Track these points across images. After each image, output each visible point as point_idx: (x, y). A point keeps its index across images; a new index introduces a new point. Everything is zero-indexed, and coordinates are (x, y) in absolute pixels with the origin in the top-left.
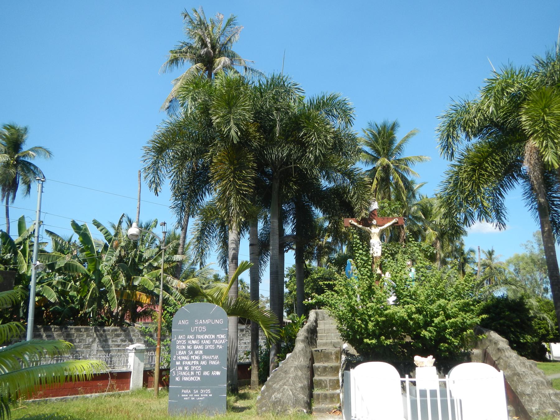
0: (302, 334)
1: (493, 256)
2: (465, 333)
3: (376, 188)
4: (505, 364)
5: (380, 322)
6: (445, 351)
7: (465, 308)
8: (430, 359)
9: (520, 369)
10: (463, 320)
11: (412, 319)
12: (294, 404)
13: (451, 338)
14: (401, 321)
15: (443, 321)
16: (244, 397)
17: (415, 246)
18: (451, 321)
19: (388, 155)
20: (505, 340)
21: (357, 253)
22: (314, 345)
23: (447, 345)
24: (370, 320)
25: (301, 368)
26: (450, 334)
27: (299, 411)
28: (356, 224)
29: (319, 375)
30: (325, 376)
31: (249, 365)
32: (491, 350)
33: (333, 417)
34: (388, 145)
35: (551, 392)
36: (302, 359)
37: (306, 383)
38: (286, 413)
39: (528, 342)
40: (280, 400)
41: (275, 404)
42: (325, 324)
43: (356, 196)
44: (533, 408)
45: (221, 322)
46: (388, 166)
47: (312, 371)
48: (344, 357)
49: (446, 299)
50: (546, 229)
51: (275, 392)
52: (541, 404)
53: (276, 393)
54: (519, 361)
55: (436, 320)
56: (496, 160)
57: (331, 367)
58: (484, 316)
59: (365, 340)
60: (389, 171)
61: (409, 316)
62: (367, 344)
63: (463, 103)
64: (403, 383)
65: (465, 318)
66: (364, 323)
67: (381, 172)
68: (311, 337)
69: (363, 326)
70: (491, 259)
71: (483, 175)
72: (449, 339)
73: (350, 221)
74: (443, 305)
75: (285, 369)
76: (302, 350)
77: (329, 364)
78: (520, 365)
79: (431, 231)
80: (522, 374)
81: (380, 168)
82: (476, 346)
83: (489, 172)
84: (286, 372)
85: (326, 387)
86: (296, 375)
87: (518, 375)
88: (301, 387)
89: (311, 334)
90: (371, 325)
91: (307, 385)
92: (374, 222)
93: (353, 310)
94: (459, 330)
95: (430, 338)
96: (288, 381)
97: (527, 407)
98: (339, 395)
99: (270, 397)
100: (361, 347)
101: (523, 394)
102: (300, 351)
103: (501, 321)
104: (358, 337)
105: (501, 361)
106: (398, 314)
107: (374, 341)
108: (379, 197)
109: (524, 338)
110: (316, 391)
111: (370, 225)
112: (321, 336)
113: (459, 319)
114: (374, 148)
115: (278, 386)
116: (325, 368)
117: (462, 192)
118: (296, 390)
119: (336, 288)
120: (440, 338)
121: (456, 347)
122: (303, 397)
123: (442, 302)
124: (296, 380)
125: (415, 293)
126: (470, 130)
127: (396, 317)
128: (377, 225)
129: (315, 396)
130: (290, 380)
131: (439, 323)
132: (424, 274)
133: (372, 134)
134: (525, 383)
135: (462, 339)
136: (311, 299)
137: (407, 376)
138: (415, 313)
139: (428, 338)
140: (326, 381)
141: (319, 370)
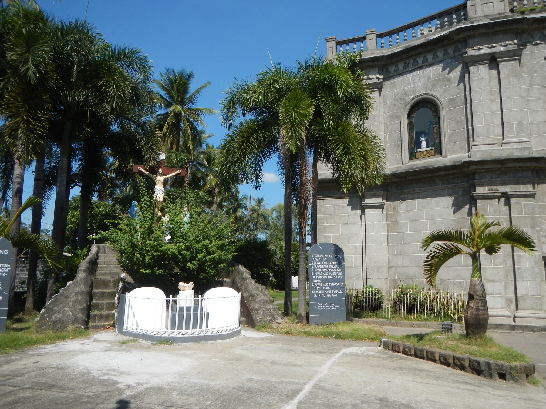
0: (84, 264)
1: (262, 204)
2: (220, 266)
3: (166, 132)
4: (245, 289)
5: (155, 256)
6: (203, 279)
7: (222, 247)
8: (191, 284)
9: (254, 292)
10: (219, 256)
11: (181, 254)
12: (73, 323)
13: (209, 269)
14: (172, 256)
15: (205, 257)
16: (19, 321)
17: (191, 197)
18: (210, 257)
19: (182, 103)
20: (248, 271)
21: (142, 198)
22: (94, 275)
23: (205, 275)
24: (147, 255)
25: (81, 293)
26: (209, 266)
27: (77, 327)
28: (143, 170)
29: (97, 300)
30: (103, 300)
31: (25, 293)
32: (237, 279)
33: (107, 331)
34: (182, 93)
35: (271, 307)
36: (82, 286)
37: (85, 305)
38: (65, 329)
39: (264, 273)
40: (60, 320)
41: (55, 323)
42: (105, 256)
43: (146, 146)
44: (258, 318)
45: (6, 253)
46: (180, 113)
47: (91, 296)
48: (121, 284)
49: (209, 240)
50: (288, 192)
51: (55, 313)
52: (263, 315)
53: (56, 315)
54: (255, 287)
55: (199, 256)
56: (260, 137)
57: (109, 293)
58: (234, 254)
59: (141, 270)
60: (181, 118)
61: (179, 252)
62: (143, 273)
63: (244, 84)
64: (168, 302)
65: (221, 255)
66: (142, 256)
67: (172, 118)
68: (92, 268)
69: (141, 259)
70: (259, 206)
71: (249, 147)
72: (207, 270)
73: (139, 168)
74: (206, 244)
75: (66, 294)
76: (84, 278)
77: (107, 290)
78: (255, 289)
79: (212, 177)
80: (255, 296)
81: (172, 114)
82: (228, 276)
83: (253, 146)
84: (67, 297)
85: (102, 308)
86: (77, 299)
87: (253, 296)
88: (81, 309)
89: (92, 265)
90: (147, 259)
91: (86, 307)
92: (160, 171)
93: (134, 246)
94: (216, 263)
95: (193, 269)
96: (68, 304)
97: (254, 318)
98: (113, 314)
99: (50, 317)
100: (138, 275)
101: (253, 309)
102: (81, 279)
103: (249, 258)
104: (136, 268)
105: (243, 286)
106: (171, 250)
107: (148, 271)
108: (169, 141)
109: (262, 271)
110: (93, 312)
111: (156, 173)
112: (101, 267)
113: (216, 256)
114: (169, 93)
115: (58, 309)
116: (103, 294)
117: (233, 158)
118: (76, 311)
119: (120, 227)
120: (201, 268)
121: (212, 276)
122: (81, 316)
123: (206, 242)
124: (76, 303)
125: (186, 234)
126: (246, 108)
127: (169, 252)
128: (162, 174)
129: (92, 316)
130: (71, 303)
131: (201, 258)
132: (195, 220)
133: (168, 80)
134: (256, 302)
135: (217, 270)
136: (96, 235)
137: (171, 296)
138: (184, 250)
139: (191, 269)
140: (103, 304)
141: (98, 295)
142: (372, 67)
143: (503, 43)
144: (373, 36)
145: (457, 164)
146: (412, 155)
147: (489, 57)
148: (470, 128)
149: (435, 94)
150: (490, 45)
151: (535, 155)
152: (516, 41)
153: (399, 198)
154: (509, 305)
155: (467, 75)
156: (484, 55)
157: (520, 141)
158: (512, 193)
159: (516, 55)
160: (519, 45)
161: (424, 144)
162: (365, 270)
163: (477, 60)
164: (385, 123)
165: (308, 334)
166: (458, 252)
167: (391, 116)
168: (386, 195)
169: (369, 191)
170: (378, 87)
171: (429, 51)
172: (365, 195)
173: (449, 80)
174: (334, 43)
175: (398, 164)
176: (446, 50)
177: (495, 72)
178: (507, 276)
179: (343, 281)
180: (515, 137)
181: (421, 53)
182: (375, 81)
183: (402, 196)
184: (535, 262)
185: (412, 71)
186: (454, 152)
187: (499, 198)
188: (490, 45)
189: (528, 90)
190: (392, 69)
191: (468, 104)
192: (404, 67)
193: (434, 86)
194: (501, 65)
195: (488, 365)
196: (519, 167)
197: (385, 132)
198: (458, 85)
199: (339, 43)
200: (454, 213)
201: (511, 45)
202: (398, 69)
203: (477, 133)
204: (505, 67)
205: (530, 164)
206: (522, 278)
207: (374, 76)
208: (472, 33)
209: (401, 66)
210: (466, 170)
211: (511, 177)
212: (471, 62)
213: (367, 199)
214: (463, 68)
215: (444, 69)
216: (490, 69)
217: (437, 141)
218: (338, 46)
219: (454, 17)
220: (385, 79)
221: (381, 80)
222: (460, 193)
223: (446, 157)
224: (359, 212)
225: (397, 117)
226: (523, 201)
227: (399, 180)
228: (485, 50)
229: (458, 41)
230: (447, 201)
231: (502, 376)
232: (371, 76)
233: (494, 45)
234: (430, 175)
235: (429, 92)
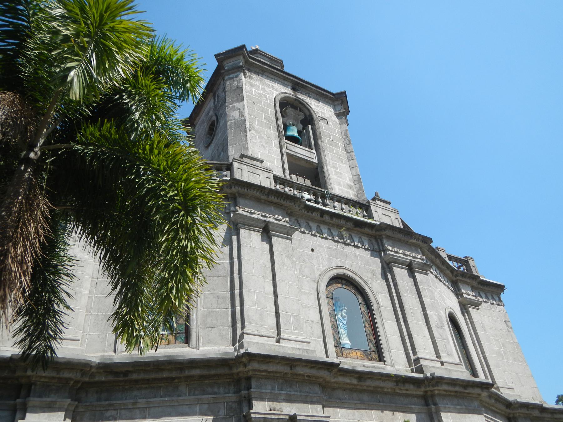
143: (276, 216)
145: (227, 357)
147: (263, 225)
148: (238, 308)
150: (263, 214)
155: (234, 238)
157: (301, 340)
158: (302, 418)
163: (250, 224)
164: (92, 278)
168: (73, 408)
169: (40, 396)
172: (30, 404)
175: (105, 351)
183: (109, 414)
186: (210, 342)
188: (263, 214)
191: (236, 276)
196: (308, 376)
197: (90, 293)
201: (284, 221)
203: (248, 317)
210: (241, 369)
211: (297, 391)
212: (242, 224)
213: (31, 412)
214: (229, 229)
222: (222, 412)
223: (197, 348)
227: (111, 378)
233: (267, 215)
234: (174, 374)
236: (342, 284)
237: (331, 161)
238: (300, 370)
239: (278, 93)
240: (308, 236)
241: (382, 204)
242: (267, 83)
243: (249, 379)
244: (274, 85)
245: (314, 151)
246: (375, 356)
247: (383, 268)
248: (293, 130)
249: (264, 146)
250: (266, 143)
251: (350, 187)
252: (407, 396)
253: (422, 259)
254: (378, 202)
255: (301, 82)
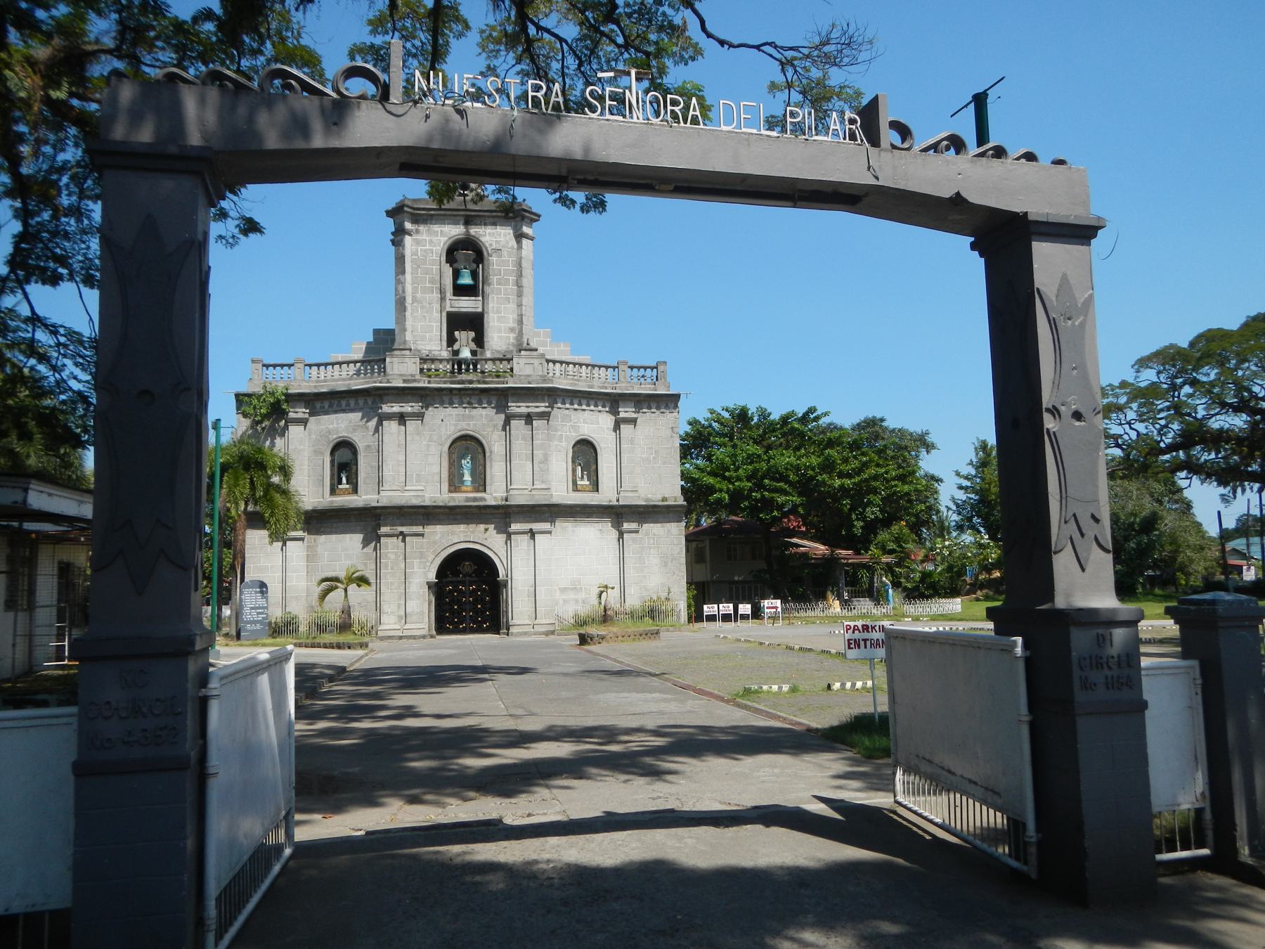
142: (299, 401)
143: (410, 404)
144: (301, 366)
146: (333, 491)
149: (354, 438)
151: (427, 503)
152: (420, 404)
153: (318, 532)
154: (400, 621)
156: (395, 413)
159: (420, 416)
160: (422, 407)
161: (344, 480)
162: (284, 598)
163: (390, 417)
165: (241, 645)
166: (337, 587)
167: (315, 451)
170: (304, 422)
171: (351, 397)
173: (367, 428)
174: (261, 365)
176: (366, 399)
177: (403, 428)
178: (400, 599)
179: (267, 608)
180: (414, 485)
181: (345, 397)
182: (300, 415)
184: (421, 587)
185: (336, 412)
187: (397, 536)
189: (428, 446)
190: (318, 405)
192: (331, 406)
193: (354, 430)
194: (408, 423)
195: (343, 643)
198: (374, 434)
199: (267, 366)
200: (363, 548)
202: (324, 407)
204: (412, 425)
205: (420, 510)
206: (410, 600)
207: (301, 410)
208: (386, 392)
209: (326, 404)
215: (362, 419)
216: (399, 425)
217: (355, 481)
218: (265, 368)
219: (376, 367)
220: (311, 414)
221: (307, 416)
222: (369, 530)
224: (280, 544)
225: (322, 453)
226: (415, 539)
228: (396, 408)
229: (375, 395)
230: (359, 537)
231: (349, 648)
232: (297, 410)
235: (350, 435)
236: (466, 440)
237: (496, 305)
238: (405, 510)
239: (446, 239)
240: (441, 409)
241: (528, 353)
242: (436, 229)
243: (380, 515)
244: (443, 229)
245: (480, 298)
246: (481, 488)
247: (505, 421)
248: (463, 276)
249: (424, 317)
250: (427, 312)
251: (512, 330)
252: (492, 514)
253: (546, 407)
254: (523, 353)
255: (473, 213)
